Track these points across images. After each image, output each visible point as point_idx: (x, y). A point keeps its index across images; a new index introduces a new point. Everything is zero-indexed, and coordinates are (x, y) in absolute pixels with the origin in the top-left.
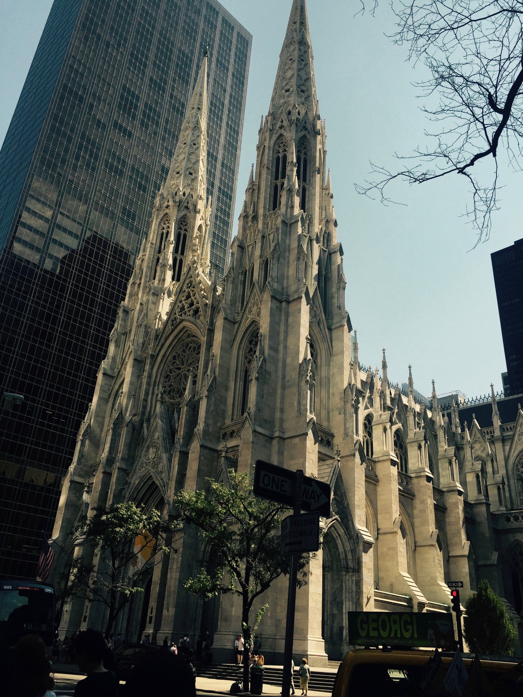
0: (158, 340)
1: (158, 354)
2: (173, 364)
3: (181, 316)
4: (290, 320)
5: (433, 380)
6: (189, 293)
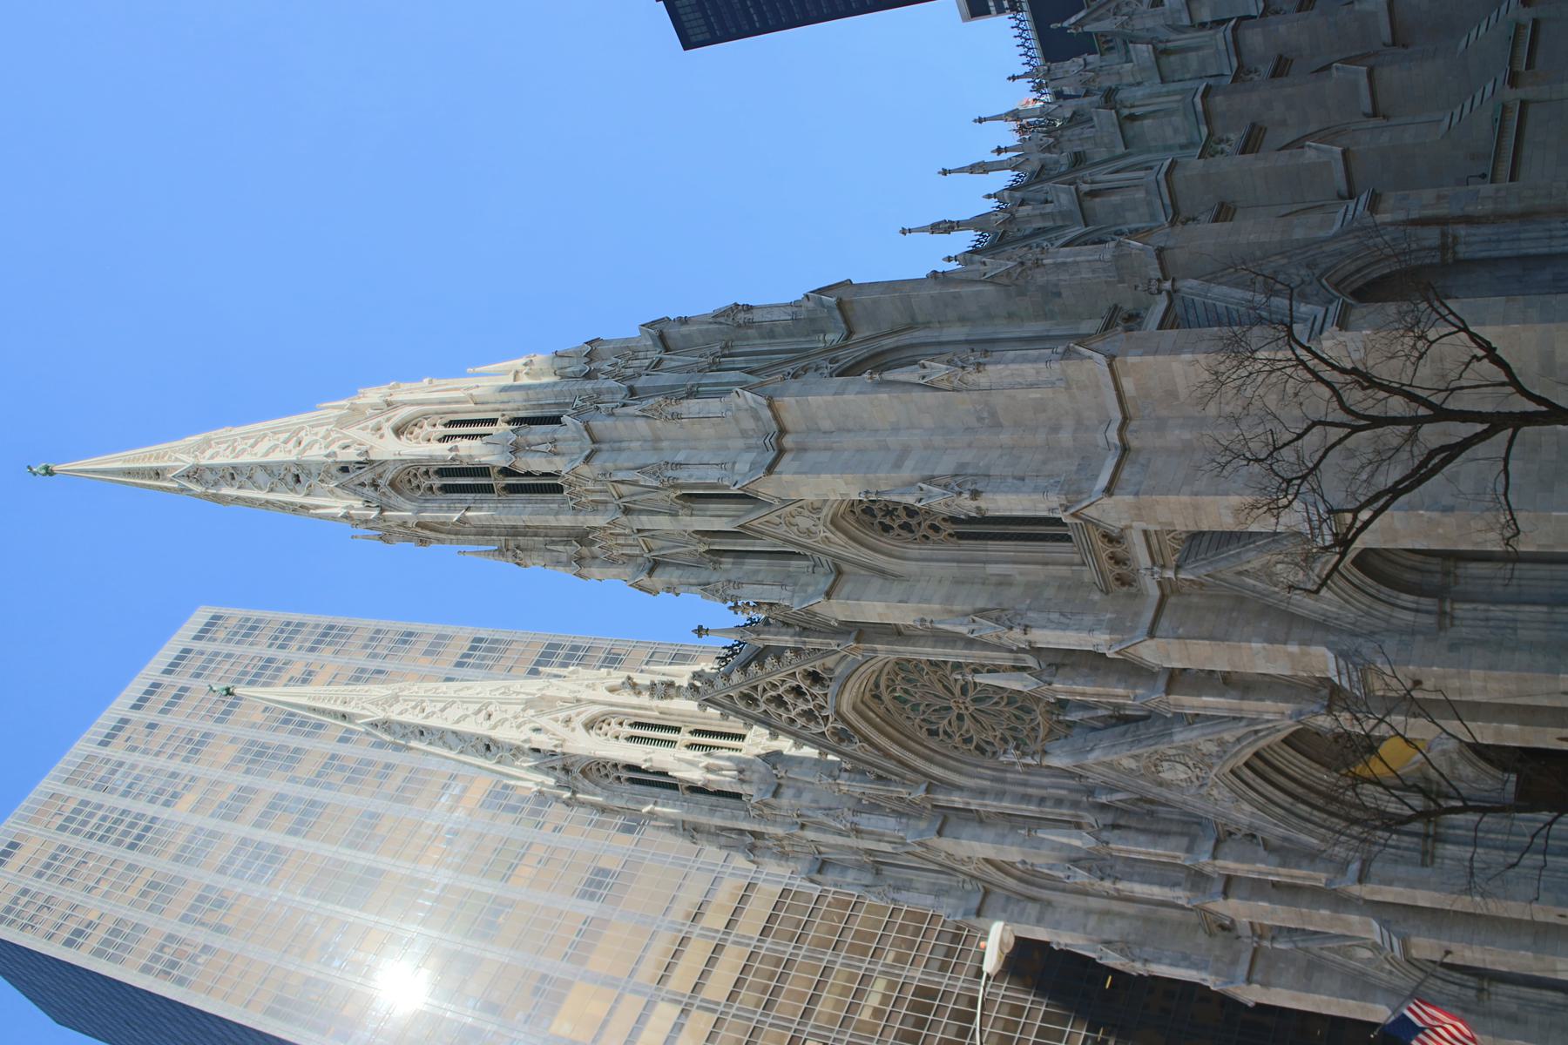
0: (890, 776)
1: (926, 775)
2: (950, 736)
3: (827, 717)
4: (826, 425)
5: (975, 121)
6: (769, 701)
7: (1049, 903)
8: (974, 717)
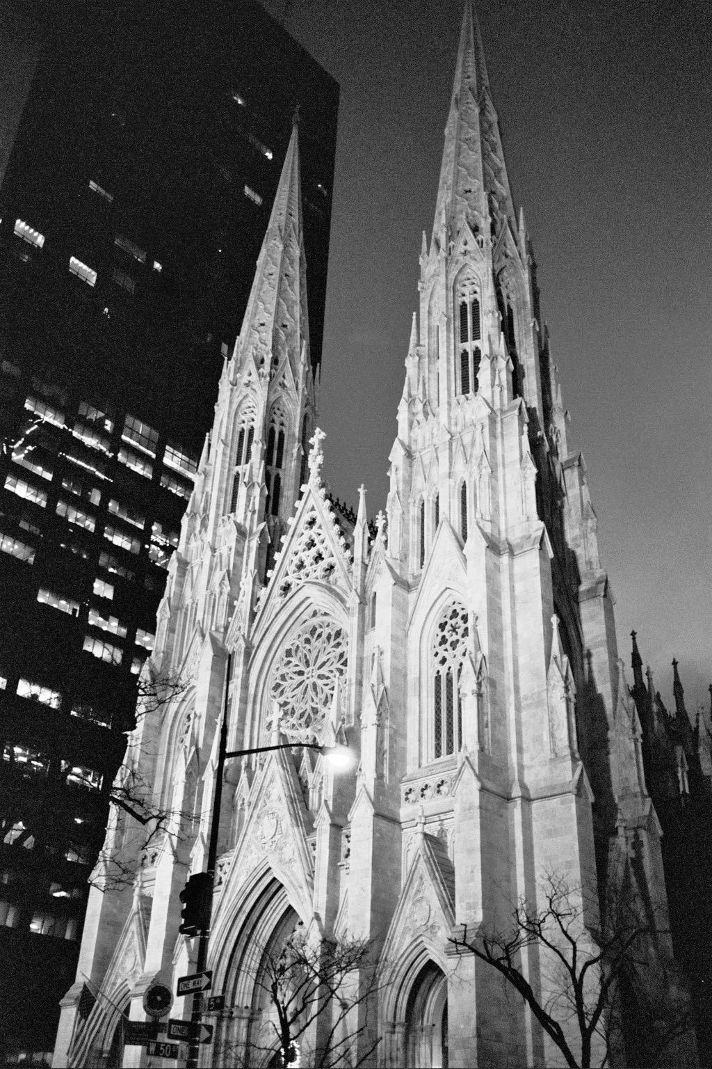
8: (301, 683)
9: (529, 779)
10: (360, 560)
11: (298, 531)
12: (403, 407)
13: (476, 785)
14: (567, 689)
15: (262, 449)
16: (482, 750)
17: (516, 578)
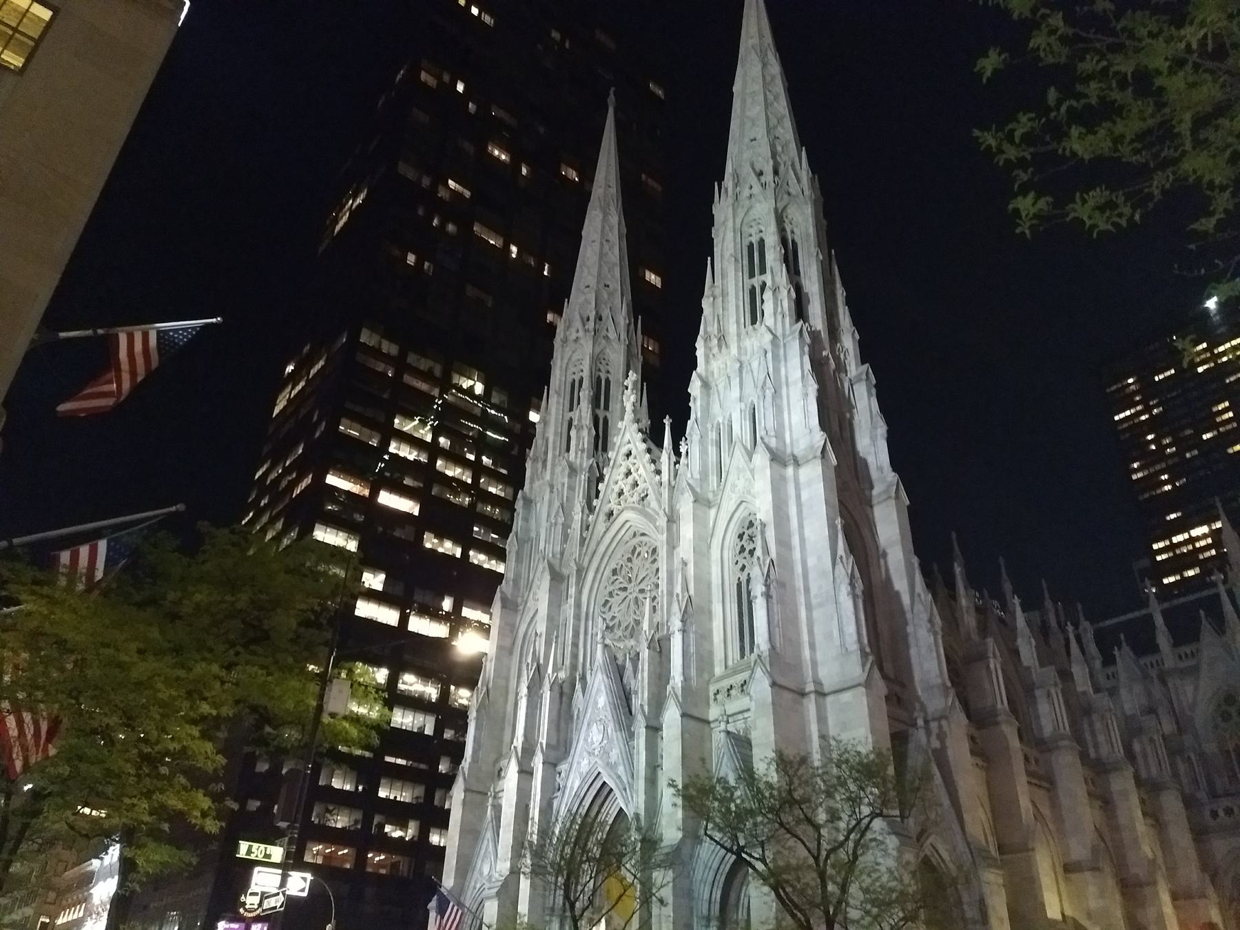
0: (586, 546)
7: (511, 653)
9: (823, 673)
10: (667, 483)
11: (618, 463)
12: (700, 345)
13: (766, 683)
14: (852, 584)
15: (589, 394)
16: (773, 648)
17: (802, 487)
